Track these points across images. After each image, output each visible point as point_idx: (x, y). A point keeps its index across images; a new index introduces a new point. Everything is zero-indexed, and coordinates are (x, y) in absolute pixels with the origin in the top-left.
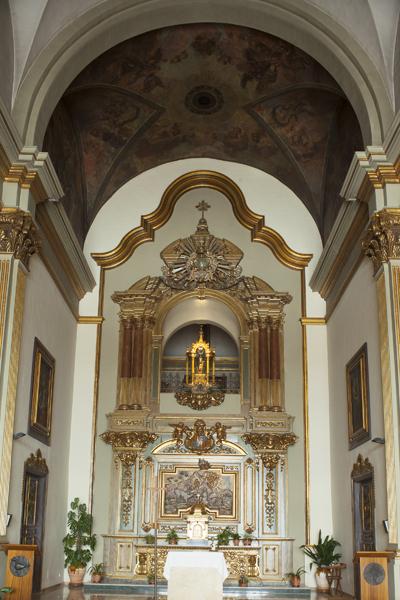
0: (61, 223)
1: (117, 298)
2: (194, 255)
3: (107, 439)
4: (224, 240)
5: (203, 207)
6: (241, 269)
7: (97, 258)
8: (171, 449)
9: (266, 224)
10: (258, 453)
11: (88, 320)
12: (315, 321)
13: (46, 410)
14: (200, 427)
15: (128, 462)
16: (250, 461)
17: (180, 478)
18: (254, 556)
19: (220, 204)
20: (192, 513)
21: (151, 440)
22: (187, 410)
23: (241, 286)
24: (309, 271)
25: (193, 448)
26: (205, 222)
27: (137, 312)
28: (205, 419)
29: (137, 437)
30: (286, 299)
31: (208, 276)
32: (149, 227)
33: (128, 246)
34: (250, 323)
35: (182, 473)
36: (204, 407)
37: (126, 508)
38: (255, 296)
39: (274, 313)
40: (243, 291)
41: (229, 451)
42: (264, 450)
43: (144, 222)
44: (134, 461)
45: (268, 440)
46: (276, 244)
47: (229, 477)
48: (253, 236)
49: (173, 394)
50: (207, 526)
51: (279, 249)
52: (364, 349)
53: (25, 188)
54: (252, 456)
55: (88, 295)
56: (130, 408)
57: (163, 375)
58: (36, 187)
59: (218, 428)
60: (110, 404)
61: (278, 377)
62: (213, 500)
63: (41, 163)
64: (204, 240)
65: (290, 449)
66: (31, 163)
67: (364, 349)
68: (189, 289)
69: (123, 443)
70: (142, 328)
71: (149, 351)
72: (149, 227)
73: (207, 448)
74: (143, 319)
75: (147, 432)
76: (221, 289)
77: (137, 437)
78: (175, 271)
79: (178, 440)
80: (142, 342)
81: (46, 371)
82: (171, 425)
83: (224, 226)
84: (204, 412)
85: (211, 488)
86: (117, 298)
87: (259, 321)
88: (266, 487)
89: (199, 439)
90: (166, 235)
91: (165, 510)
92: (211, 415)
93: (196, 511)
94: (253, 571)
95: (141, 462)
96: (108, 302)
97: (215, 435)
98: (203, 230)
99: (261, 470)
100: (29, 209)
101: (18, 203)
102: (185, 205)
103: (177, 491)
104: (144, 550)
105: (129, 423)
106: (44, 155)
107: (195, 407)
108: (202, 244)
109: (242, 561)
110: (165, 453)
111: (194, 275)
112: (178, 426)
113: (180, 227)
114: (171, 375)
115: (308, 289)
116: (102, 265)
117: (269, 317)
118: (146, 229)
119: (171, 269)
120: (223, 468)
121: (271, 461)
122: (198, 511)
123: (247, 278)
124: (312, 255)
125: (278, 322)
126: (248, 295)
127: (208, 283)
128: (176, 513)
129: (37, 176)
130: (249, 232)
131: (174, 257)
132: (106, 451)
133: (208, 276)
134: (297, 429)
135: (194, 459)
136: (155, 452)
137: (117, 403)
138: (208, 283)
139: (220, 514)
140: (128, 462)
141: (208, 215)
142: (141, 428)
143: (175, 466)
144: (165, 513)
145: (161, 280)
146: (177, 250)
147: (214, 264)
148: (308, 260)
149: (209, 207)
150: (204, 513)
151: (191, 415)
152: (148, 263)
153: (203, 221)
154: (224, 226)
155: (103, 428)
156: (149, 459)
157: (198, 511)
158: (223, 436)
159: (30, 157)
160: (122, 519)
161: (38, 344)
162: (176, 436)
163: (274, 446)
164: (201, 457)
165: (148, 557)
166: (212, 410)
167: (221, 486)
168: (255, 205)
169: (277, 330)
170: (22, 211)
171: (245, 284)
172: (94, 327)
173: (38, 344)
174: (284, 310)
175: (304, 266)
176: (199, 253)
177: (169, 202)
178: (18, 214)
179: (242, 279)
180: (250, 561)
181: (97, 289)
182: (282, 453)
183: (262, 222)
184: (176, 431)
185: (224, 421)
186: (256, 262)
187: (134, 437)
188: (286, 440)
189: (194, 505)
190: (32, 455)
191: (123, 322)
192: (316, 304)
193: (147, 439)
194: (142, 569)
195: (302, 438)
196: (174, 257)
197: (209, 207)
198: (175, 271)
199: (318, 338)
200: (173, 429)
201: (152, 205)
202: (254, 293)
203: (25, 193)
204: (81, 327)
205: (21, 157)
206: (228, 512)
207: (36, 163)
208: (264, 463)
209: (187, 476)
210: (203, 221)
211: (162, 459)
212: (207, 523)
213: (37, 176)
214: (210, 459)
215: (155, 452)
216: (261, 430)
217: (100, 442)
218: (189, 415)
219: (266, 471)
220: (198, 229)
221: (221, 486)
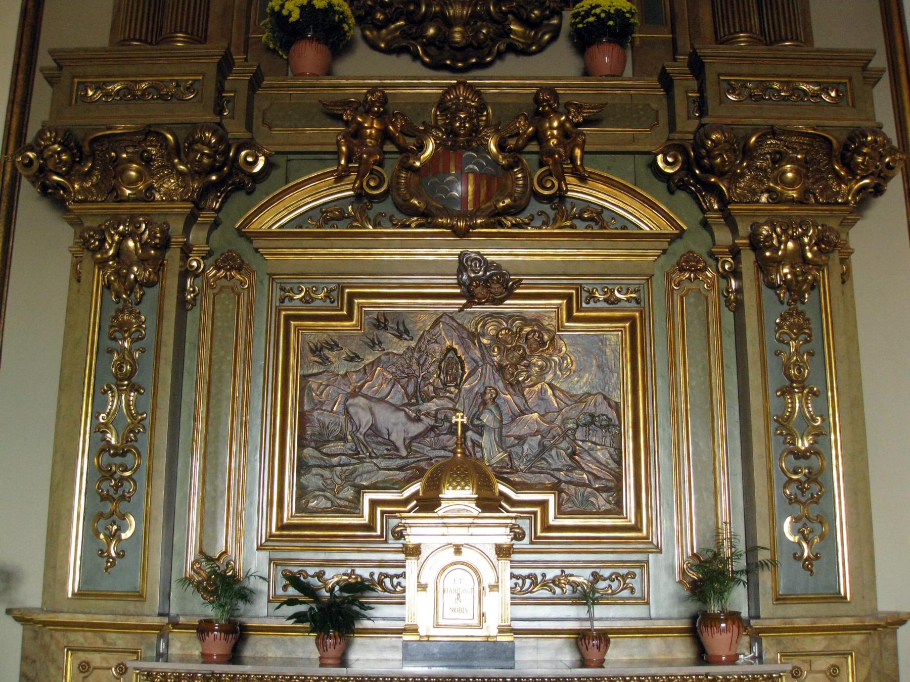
17: (374, 344)
20: (428, 503)
91: (302, 492)
128: (354, 507)
144: (302, 509)
150: (489, 503)
206: (601, 501)
209: (402, 333)
212: (503, 552)
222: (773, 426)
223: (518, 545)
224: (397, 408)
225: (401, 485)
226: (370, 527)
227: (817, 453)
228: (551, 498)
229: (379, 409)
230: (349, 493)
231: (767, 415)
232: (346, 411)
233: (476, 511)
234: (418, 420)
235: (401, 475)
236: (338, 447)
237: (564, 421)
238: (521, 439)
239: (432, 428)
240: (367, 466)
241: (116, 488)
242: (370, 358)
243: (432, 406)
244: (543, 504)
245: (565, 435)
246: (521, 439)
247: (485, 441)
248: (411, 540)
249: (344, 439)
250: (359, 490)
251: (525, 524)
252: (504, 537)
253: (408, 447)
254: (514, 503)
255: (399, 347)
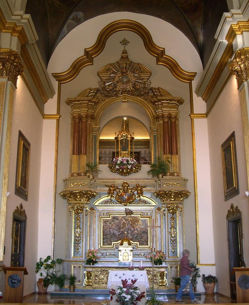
0: (36, 55)
1: (69, 102)
2: (119, 74)
3: (64, 196)
4: (139, 64)
5: (125, 42)
6: (150, 83)
7: (56, 76)
8: (106, 202)
9: (166, 54)
10: (164, 204)
11: (50, 117)
12: (200, 116)
13: (25, 177)
14: (125, 186)
15: (79, 211)
16: (159, 209)
17: (113, 221)
18: (163, 272)
19: (136, 40)
20: (122, 244)
21: (94, 196)
22: (117, 176)
23: (151, 94)
24: (195, 84)
25: (121, 201)
26: (126, 53)
27: (83, 111)
28: (129, 182)
29: (84, 194)
30: (180, 102)
31: (129, 87)
32: (90, 55)
33: (76, 68)
34: (157, 118)
35: (114, 218)
36: (128, 173)
37: (77, 242)
38: (160, 100)
39: (173, 111)
40: (152, 97)
41: (145, 202)
42: (169, 201)
43: (87, 53)
44: (82, 210)
45: (171, 195)
46: (173, 67)
47: (145, 220)
48: (158, 61)
49: (107, 165)
50: (132, 252)
51: (175, 69)
52: (233, 135)
53: (15, 36)
54: (160, 206)
55: (50, 100)
56: (79, 174)
57: (100, 153)
58: (22, 35)
59: (138, 187)
60: (65, 174)
61: (177, 153)
62: (136, 235)
63: (26, 21)
64: (126, 64)
65: (185, 200)
66: (19, 21)
67: (233, 135)
68: (116, 95)
69: (74, 199)
70: (86, 122)
71: (91, 137)
72: (89, 56)
73: (130, 200)
74: (87, 116)
75: (91, 191)
76: (138, 96)
77: (84, 194)
78: (107, 84)
79: (112, 196)
80: (86, 131)
81: (25, 149)
82: (106, 186)
83: (138, 53)
84: (128, 177)
85: (133, 227)
86: (69, 102)
87: (163, 116)
88: (170, 226)
89: (126, 195)
90: (102, 61)
91: (103, 242)
92: (133, 179)
93: (124, 243)
94: (162, 282)
95: (87, 211)
96: (63, 106)
97: (136, 192)
98: (125, 57)
99: (166, 215)
100: (17, 49)
101: (10, 46)
102: (114, 40)
103: (111, 230)
104: (90, 270)
105: (76, 186)
106: (28, 16)
107: (122, 173)
108: (126, 65)
109: (155, 276)
110: (106, 207)
111: (120, 87)
112: (111, 186)
113: (111, 55)
114: (105, 152)
115: (194, 95)
116: (59, 81)
117: (170, 114)
118: (87, 57)
119: (104, 83)
120: (143, 214)
121: (173, 209)
122: (126, 243)
123: (154, 88)
124: (196, 73)
125: (176, 117)
126: (155, 99)
127: (128, 92)
128: (111, 244)
129: (23, 28)
130: (156, 58)
131: (105, 76)
132: (63, 202)
133: (129, 87)
134: (190, 188)
135: (121, 208)
136: (95, 205)
137: (70, 171)
138: (128, 92)
139: (140, 245)
140: (79, 211)
141: (128, 48)
142: (87, 189)
143: (108, 214)
144: (103, 245)
145: (98, 90)
146: (108, 70)
147: (133, 80)
148: (194, 76)
149: (129, 42)
150: (130, 244)
151: (120, 179)
152: (89, 79)
153: (125, 52)
154: (138, 53)
155: (61, 189)
156: (92, 209)
157: (126, 243)
158: (141, 193)
159: (19, 18)
160: (75, 248)
161: (21, 135)
162: (109, 193)
163: (176, 199)
164: (127, 207)
165: (93, 274)
166: (133, 176)
167: (140, 226)
168: (159, 41)
169: (175, 122)
170: (13, 51)
171: (153, 92)
172: (54, 122)
173: (21, 135)
174: (179, 109)
175: (191, 80)
176: (122, 73)
177: (103, 40)
178: (11, 53)
179: (151, 89)
180: (160, 275)
181: (56, 96)
182: (180, 204)
183: (163, 52)
184: (110, 190)
185: (141, 183)
186: (160, 79)
187: (82, 194)
188: (182, 195)
189: (122, 238)
190: (17, 207)
191: (74, 118)
192: (200, 105)
193: (91, 196)
194: (88, 282)
195: (193, 194)
196: (105, 76)
197: (129, 42)
198: (107, 84)
199: (201, 127)
200: (107, 189)
201: (91, 41)
202: (159, 98)
203: (15, 39)
204: (46, 122)
205: (13, 17)
206: (145, 243)
207: (23, 21)
208: (169, 210)
209: (117, 219)
210: (125, 52)
211: (101, 208)
212: (131, 251)
213: (23, 28)
214: (131, 208)
215: (96, 204)
216: (165, 187)
217: (60, 199)
218: (119, 180)
219: (170, 215)
220: (122, 57)
221: (140, 226)
222: (169, 233)
223: (134, 250)
224: (117, 230)
225: (117, 241)
226: (113, 247)
227: (175, 237)
228: (138, 243)
229: (114, 231)
230: (110, 242)
231: (168, 231)
232: (110, 231)
233: (128, 245)
234: (120, 232)
235: (117, 240)
236: (109, 236)
237: (140, 232)
238: (134, 235)
239: (121, 233)
240: (113, 238)
241: (78, 242)
242: (113, 223)
243: (121, 230)
244: (137, 244)
245: (140, 234)
246: (134, 235)
247: (129, 235)
248: (120, 249)
249: (109, 235)
250: (111, 242)
251: (134, 247)
252: (132, 249)
253: (118, 236)
254: (133, 244)
255: (117, 221)
